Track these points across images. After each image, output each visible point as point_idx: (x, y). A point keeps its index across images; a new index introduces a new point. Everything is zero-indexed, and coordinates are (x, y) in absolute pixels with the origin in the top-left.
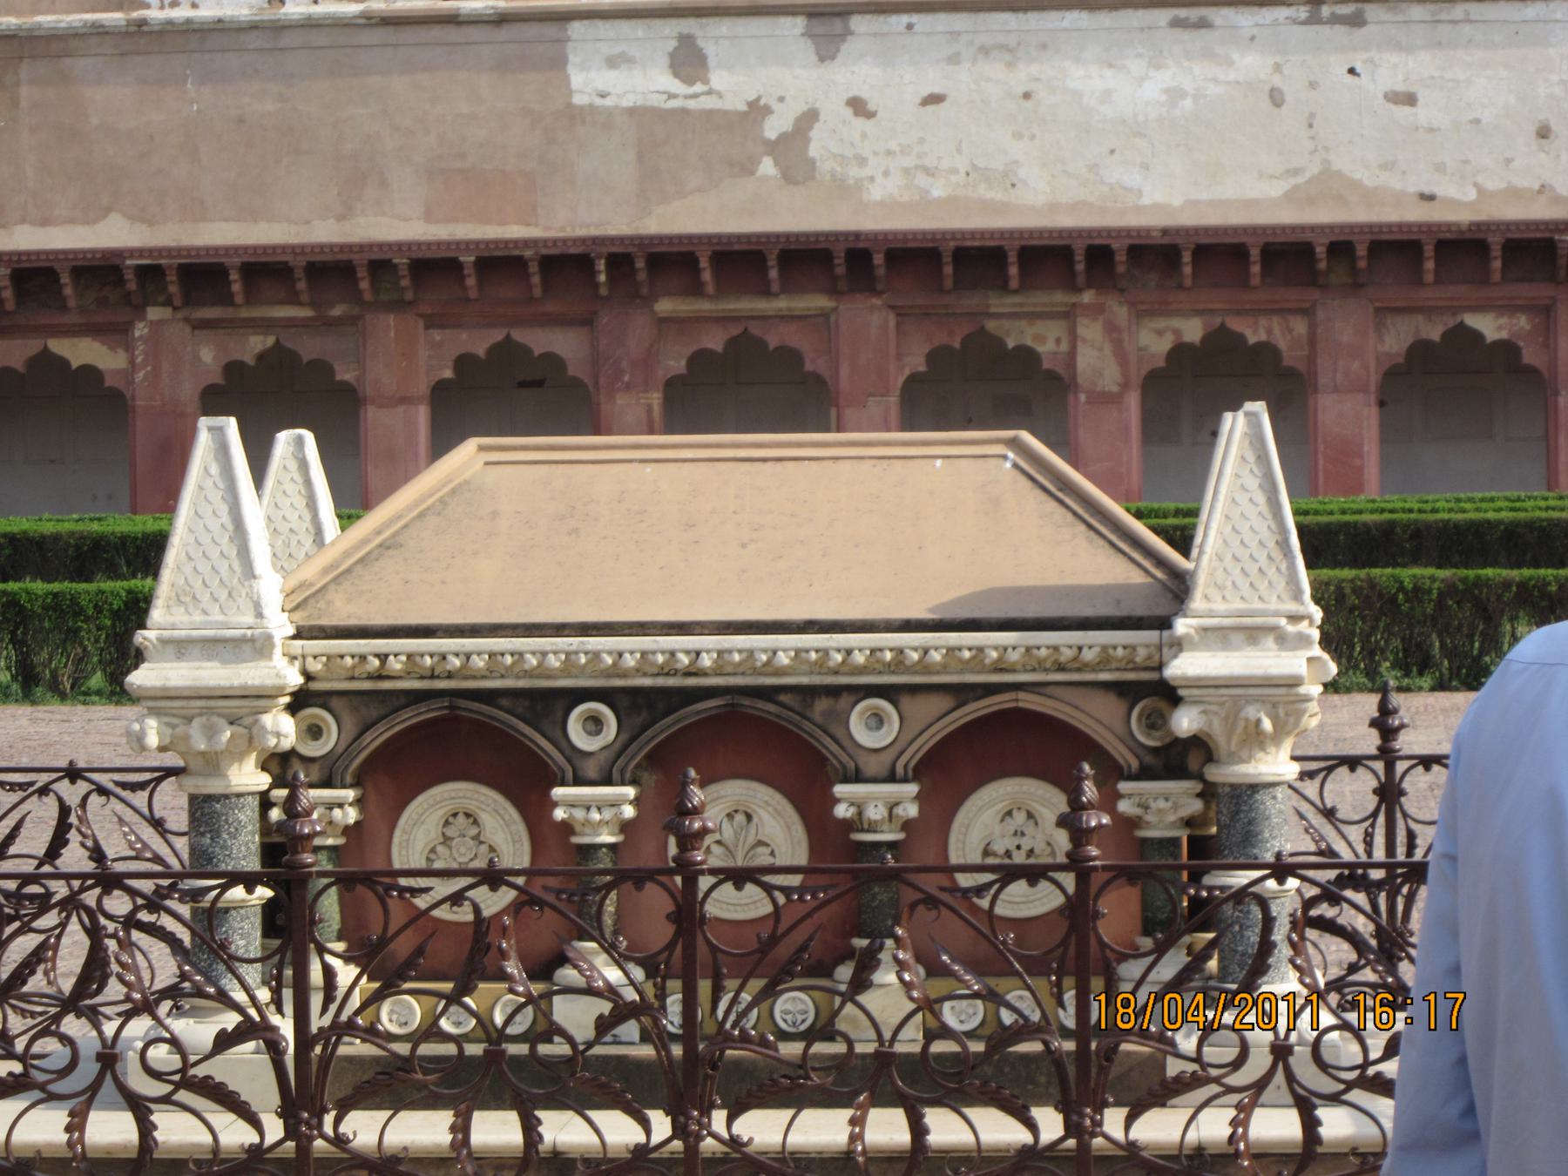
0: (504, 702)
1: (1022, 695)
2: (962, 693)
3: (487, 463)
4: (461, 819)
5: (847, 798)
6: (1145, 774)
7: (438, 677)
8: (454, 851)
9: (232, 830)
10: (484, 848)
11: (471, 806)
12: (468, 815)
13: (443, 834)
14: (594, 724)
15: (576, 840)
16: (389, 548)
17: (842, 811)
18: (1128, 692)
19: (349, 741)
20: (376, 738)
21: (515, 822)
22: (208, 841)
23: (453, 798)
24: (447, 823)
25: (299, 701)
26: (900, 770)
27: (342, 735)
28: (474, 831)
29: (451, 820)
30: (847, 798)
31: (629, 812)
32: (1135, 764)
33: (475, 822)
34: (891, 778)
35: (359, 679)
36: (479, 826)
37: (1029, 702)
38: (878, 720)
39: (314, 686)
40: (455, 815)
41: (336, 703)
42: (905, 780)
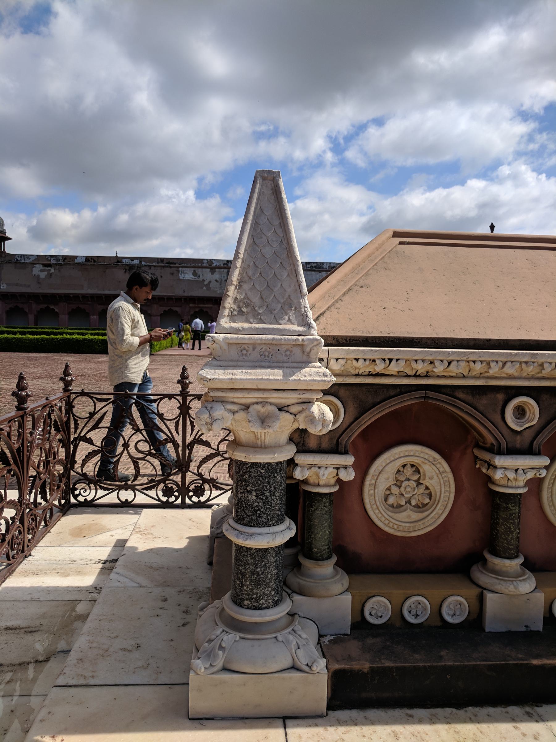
0: (461, 395)
3: (401, 243)
4: (408, 467)
7: (419, 376)
8: (402, 489)
9: (273, 489)
10: (422, 489)
11: (415, 460)
12: (412, 466)
13: (396, 477)
14: (520, 412)
16: (361, 287)
19: (352, 420)
20: (368, 419)
21: (445, 472)
22: (254, 498)
23: (406, 456)
24: (399, 471)
27: (346, 415)
28: (416, 477)
29: (401, 469)
33: (418, 471)
35: (362, 375)
36: (419, 473)
40: (404, 466)
41: (342, 392)
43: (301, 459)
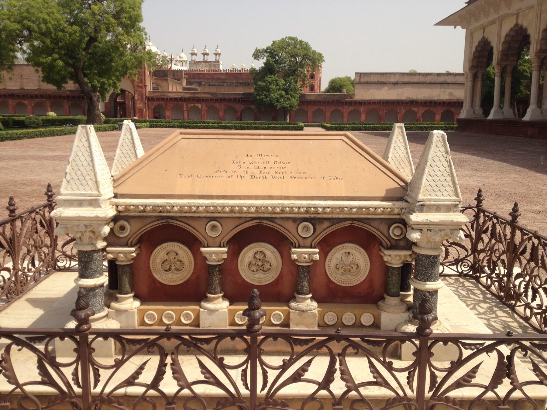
1: (355, 222)
2: (333, 221)
5: (296, 253)
6: (394, 246)
15: (207, 262)
17: (294, 257)
18: (390, 222)
25: (115, 219)
26: (313, 245)
30: (296, 253)
31: (225, 256)
32: (389, 244)
34: (311, 247)
37: (357, 224)
38: (306, 229)
39: (121, 214)
42: (315, 248)
43: (108, 249)
